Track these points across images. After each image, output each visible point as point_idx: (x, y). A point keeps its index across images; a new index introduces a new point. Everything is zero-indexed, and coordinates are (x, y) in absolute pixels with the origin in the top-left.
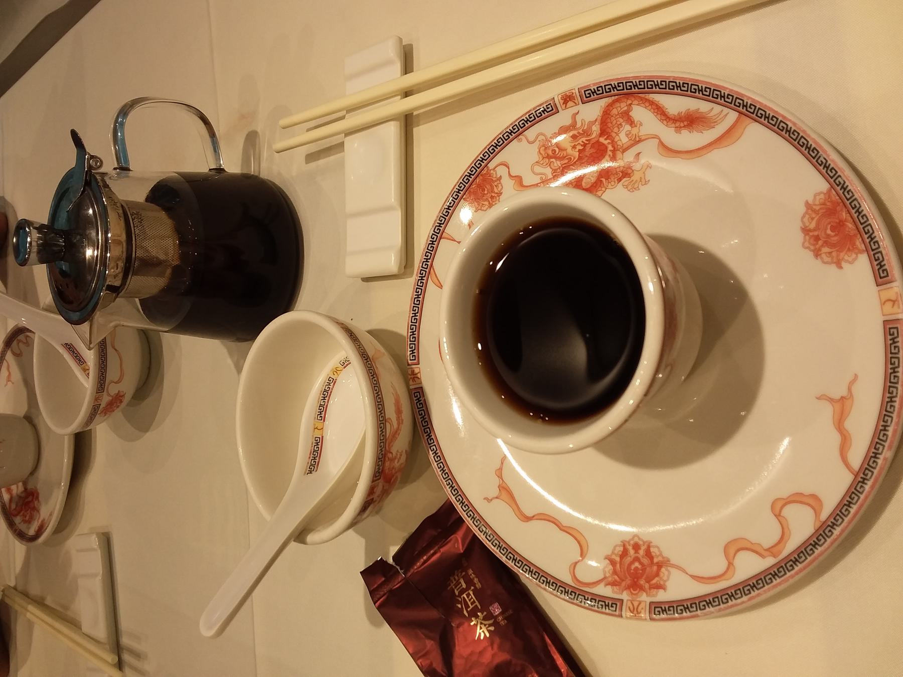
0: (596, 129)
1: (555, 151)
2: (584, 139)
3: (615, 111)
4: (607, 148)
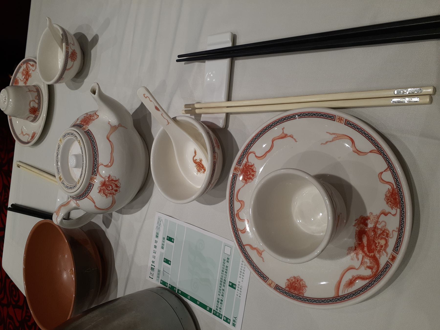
0: (377, 256)
1: (384, 236)
2: (378, 249)
3: (376, 266)
4: (369, 253)
